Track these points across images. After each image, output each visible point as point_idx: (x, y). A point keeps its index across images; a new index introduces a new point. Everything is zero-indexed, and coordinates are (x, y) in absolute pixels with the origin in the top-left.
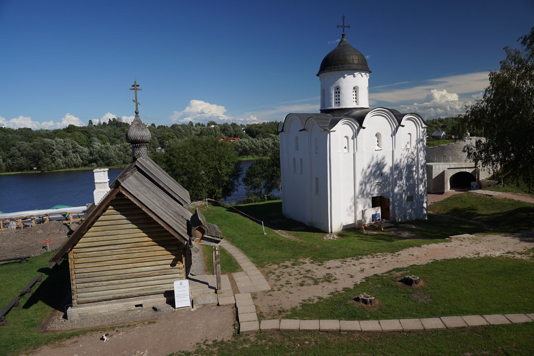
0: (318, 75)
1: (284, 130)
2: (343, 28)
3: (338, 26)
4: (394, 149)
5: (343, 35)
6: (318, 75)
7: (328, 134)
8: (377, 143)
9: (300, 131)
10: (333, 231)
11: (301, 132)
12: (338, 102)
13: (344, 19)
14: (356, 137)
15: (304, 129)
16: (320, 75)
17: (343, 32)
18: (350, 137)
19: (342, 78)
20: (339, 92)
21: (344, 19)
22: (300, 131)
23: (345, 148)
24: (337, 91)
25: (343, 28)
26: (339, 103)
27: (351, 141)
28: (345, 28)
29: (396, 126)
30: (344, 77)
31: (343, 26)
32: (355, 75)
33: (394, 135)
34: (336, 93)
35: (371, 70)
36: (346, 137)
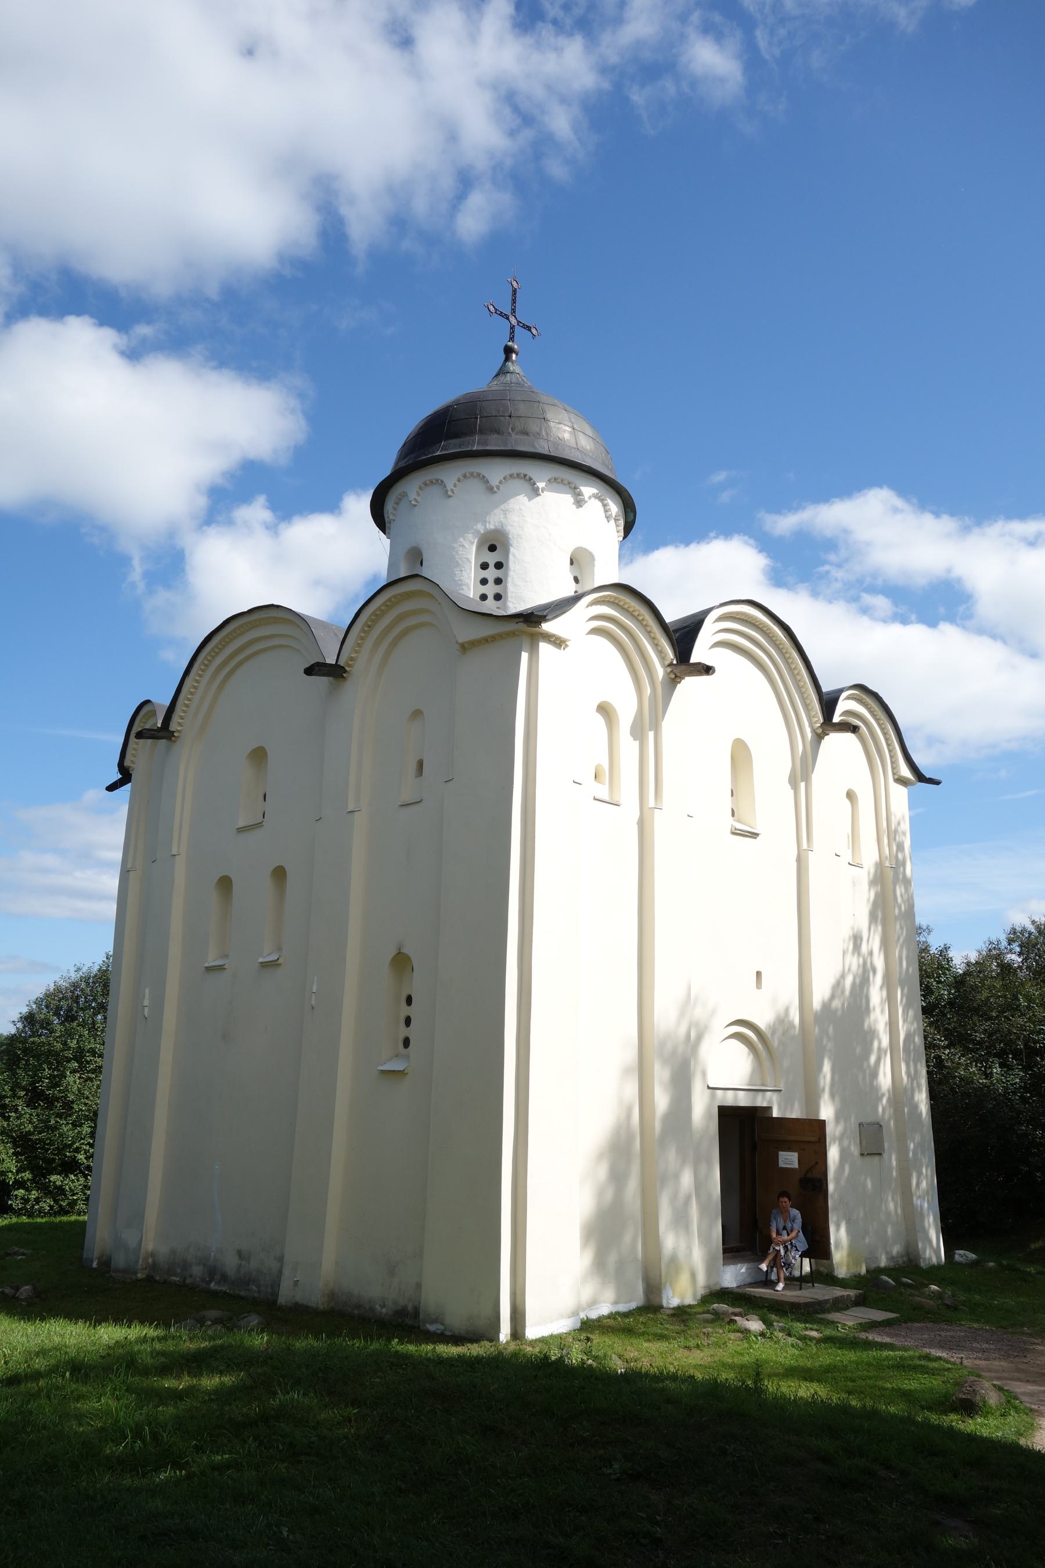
1: (173, 726)
2: (512, 328)
4: (805, 846)
5: (508, 351)
7: (525, 656)
8: (727, 803)
13: (515, 291)
14: (656, 727)
15: (336, 672)
17: (512, 339)
18: (627, 708)
19: (522, 499)
20: (499, 566)
21: (515, 291)
24: (492, 558)
27: (629, 748)
28: (518, 330)
29: (814, 731)
30: (536, 492)
32: (580, 494)
33: (806, 777)
34: (484, 566)
36: (604, 709)
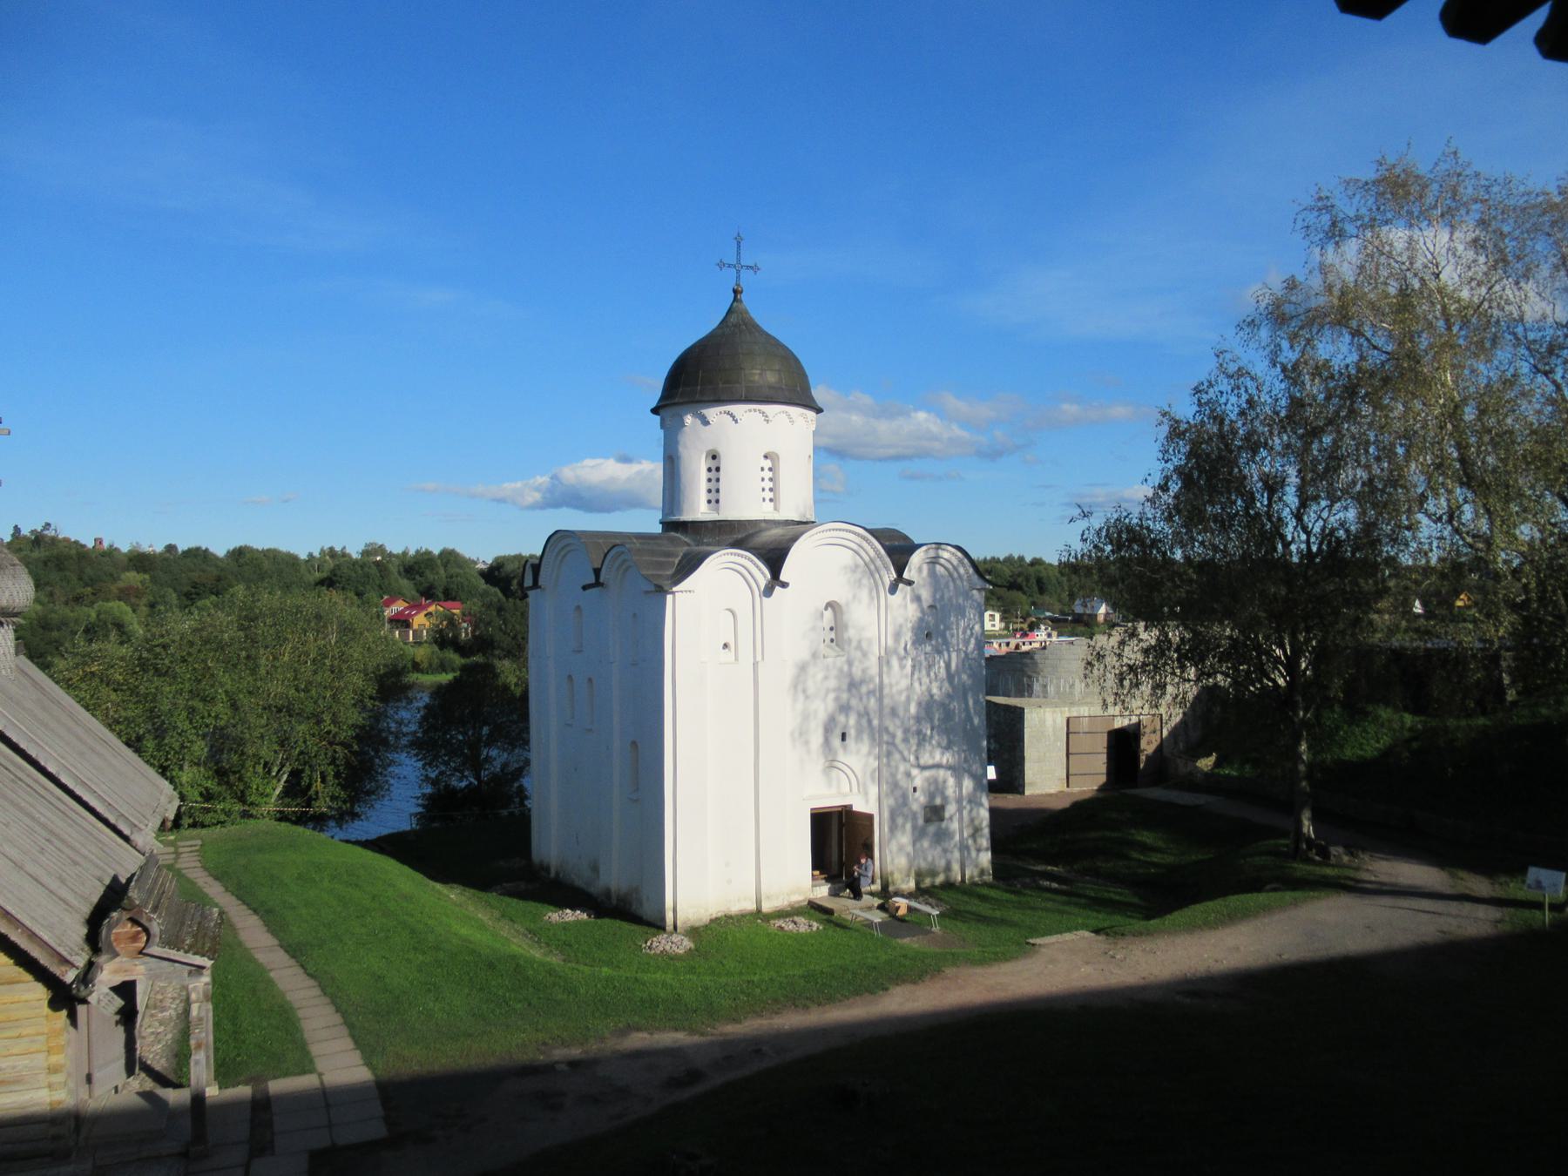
0: (655, 411)
2: (738, 272)
3: (721, 265)
5: (735, 292)
6: (655, 411)
9: (585, 588)
10: (679, 924)
11: (588, 591)
12: (714, 502)
13: (739, 243)
16: (661, 411)
20: (718, 469)
21: (739, 243)
22: (585, 588)
23: (726, 646)
25: (738, 272)
26: (717, 501)
28: (743, 271)
31: (738, 267)
34: (709, 470)
35: (820, 403)
